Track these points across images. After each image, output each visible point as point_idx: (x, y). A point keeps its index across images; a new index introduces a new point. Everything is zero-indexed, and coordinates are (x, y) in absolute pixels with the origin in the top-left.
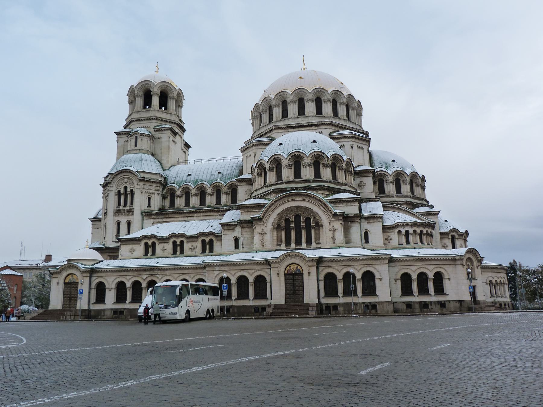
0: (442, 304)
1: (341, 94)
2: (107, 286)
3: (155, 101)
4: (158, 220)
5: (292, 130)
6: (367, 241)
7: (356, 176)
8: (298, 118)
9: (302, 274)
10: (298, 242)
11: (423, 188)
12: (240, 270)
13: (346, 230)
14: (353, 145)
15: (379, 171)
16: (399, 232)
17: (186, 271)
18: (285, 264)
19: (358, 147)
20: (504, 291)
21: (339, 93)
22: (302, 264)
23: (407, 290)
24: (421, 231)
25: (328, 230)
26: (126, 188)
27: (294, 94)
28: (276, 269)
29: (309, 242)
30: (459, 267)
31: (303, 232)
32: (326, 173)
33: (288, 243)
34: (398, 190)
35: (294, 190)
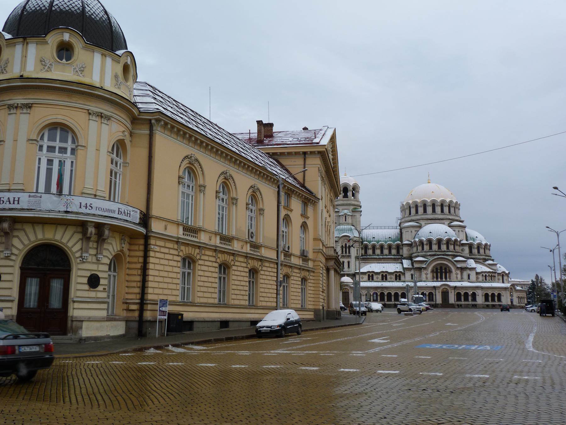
0: (500, 305)
2: (362, 294)
3: (350, 194)
4: (364, 262)
6: (469, 278)
8: (433, 214)
10: (441, 278)
11: (489, 250)
12: (423, 290)
16: (483, 275)
17: (397, 289)
18: (442, 288)
19: (461, 231)
20: (525, 301)
22: (448, 289)
23: (487, 299)
24: (492, 275)
25: (454, 274)
26: (346, 244)
29: (446, 278)
31: (444, 274)
32: (451, 247)
33: (437, 278)
34: (479, 252)
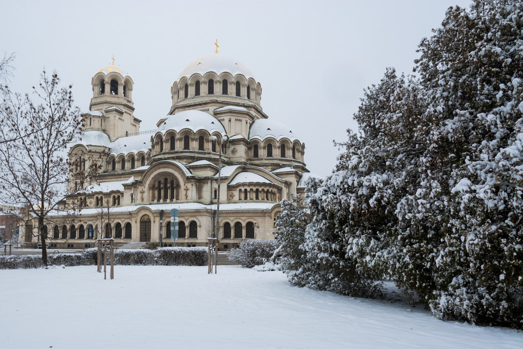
1: (229, 75)
5: (188, 108)
7: (231, 144)
9: (150, 222)
13: (199, 190)
14: (230, 118)
15: (254, 139)
16: (240, 190)
17: (91, 219)
18: (140, 215)
21: (228, 74)
27: (191, 78)
28: (135, 218)
30: (267, 219)
31: (169, 191)
35: (167, 160)
